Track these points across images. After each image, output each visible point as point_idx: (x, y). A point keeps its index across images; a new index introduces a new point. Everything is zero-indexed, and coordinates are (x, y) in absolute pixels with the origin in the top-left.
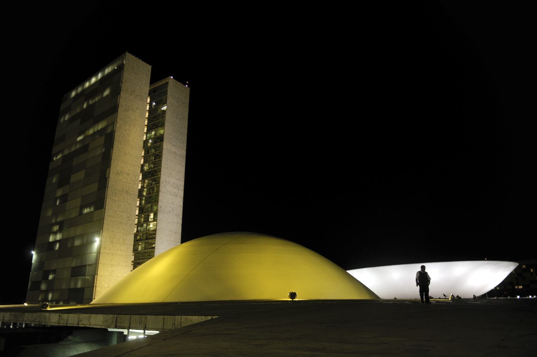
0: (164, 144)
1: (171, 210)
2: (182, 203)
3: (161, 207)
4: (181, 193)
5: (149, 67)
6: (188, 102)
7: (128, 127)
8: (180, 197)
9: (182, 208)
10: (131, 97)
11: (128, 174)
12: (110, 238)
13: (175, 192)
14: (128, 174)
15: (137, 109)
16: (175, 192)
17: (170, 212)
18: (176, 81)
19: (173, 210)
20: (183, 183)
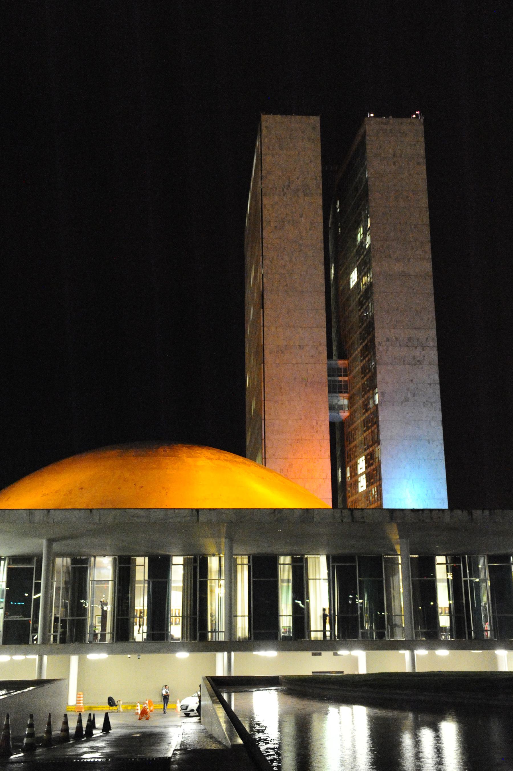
1: (409, 395)
2: (436, 377)
4: (433, 355)
5: (315, 120)
6: (422, 151)
7: (286, 258)
8: (430, 364)
9: (438, 387)
10: (285, 198)
13: (414, 358)
15: (301, 216)
16: (414, 358)
17: (407, 400)
19: (414, 395)
20: (433, 333)
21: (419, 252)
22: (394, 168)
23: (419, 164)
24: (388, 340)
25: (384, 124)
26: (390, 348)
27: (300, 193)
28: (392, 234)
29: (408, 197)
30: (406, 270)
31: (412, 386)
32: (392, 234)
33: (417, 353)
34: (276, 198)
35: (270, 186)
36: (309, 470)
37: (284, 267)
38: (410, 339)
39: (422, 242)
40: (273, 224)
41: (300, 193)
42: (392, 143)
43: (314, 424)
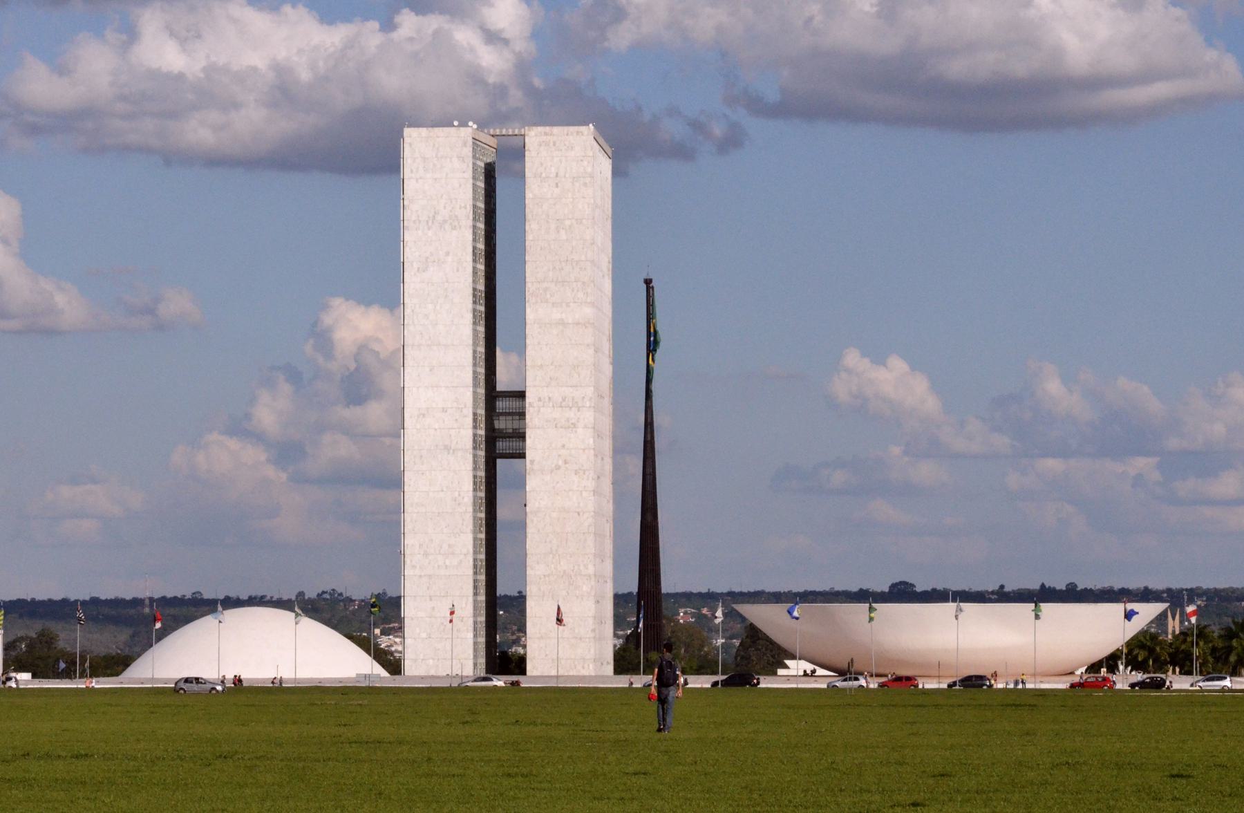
0: (528, 310)
1: (560, 463)
2: (591, 441)
3: (532, 462)
7: (430, 306)
8: (585, 427)
10: (430, 233)
11: (444, 410)
12: (421, 545)
13: (568, 420)
14: (444, 410)
15: (447, 254)
16: (568, 420)
17: (558, 468)
18: (547, 129)
19: (566, 462)
21: (580, 295)
22: (557, 191)
23: (585, 184)
24: (540, 400)
25: (546, 134)
26: (542, 410)
27: (447, 226)
28: (551, 274)
29: (570, 227)
30: (564, 316)
31: (563, 452)
32: (551, 274)
33: (571, 414)
34: (420, 232)
35: (414, 218)
36: (450, 546)
37: (426, 316)
38: (564, 400)
39: (584, 283)
40: (415, 265)
41: (447, 226)
42: (556, 160)
43: (456, 494)
